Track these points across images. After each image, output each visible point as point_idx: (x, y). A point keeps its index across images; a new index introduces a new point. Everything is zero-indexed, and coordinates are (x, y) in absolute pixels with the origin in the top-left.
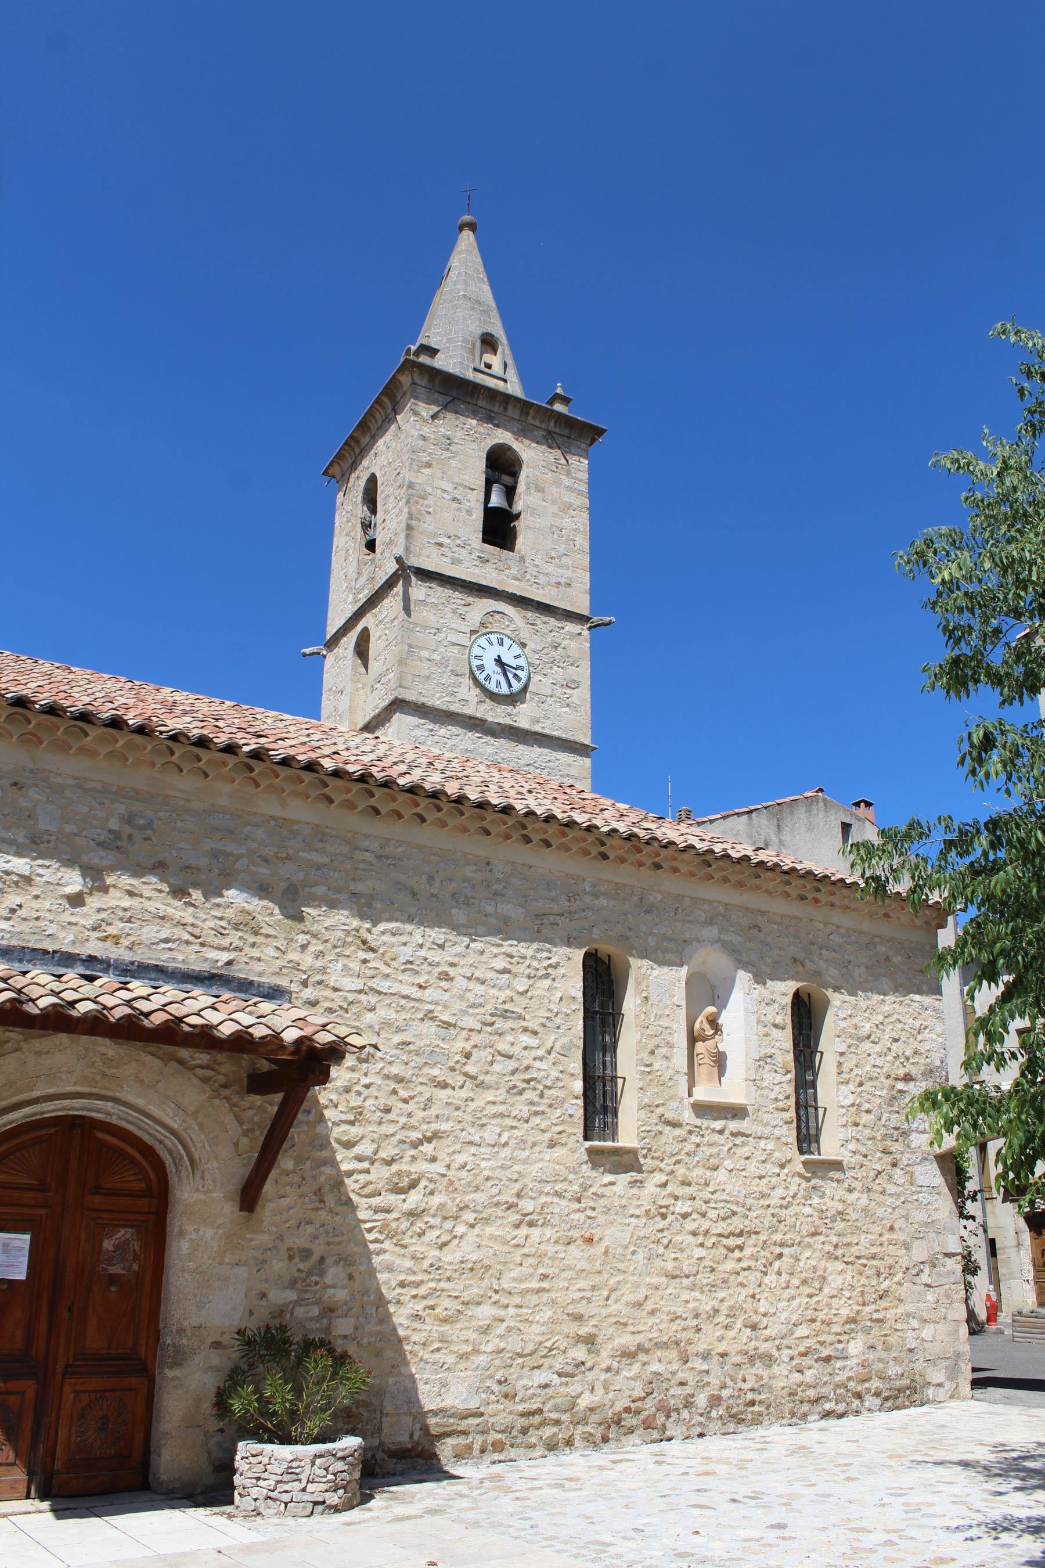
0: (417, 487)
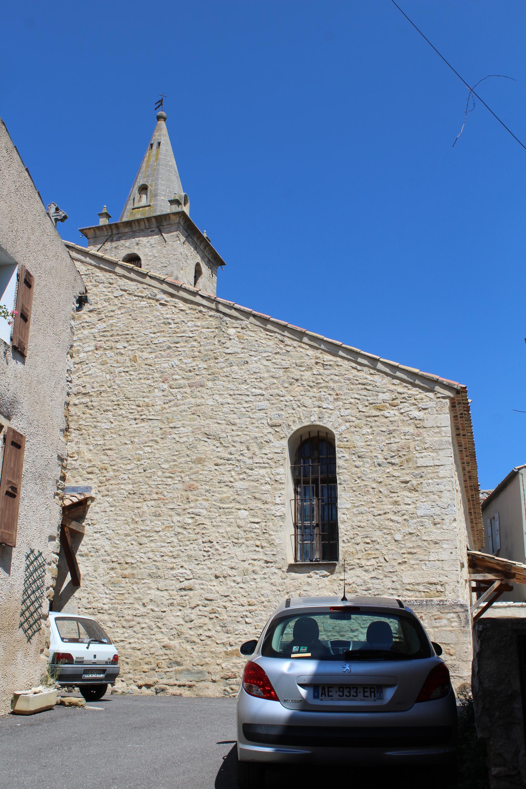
0: (179, 280)
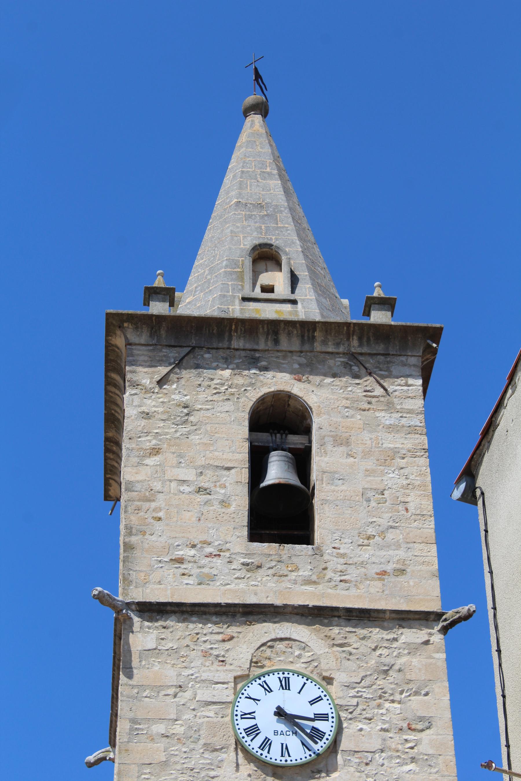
0: (138, 487)
